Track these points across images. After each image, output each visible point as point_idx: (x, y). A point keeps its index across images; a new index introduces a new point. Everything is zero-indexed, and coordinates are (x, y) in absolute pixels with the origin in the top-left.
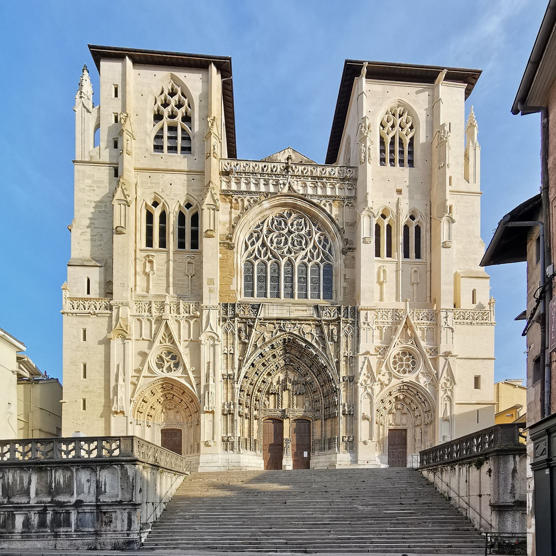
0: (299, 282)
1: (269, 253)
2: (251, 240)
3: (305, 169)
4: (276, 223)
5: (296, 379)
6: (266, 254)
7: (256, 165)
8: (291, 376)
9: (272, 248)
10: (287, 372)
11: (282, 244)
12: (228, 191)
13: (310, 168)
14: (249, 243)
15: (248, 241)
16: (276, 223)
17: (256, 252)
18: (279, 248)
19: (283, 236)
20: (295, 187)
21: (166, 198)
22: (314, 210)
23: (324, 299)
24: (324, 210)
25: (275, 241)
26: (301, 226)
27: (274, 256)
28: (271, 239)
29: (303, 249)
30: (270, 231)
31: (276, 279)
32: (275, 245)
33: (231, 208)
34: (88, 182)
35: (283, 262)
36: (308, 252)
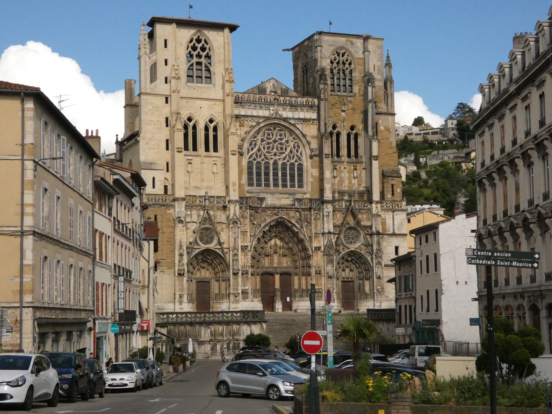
0: (282, 176)
2: (251, 147)
3: (285, 99)
4: (266, 134)
5: (282, 244)
6: (260, 156)
7: (255, 96)
8: (278, 242)
9: (264, 152)
10: (275, 240)
11: (271, 149)
12: (239, 115)
13: (288, 98)
14: (250, 148)
15: (250, 147)
16: (266, 134)
17: (254, 156)
18: (269, 153)
20: (280, 113)
21: (198, 118)
22: (292, 128)
23: (298, 188)
24: (298, 129)
25: (266, 146)
27: (266, 158)
28: (264, 146)
30: (262, 140)
31: (267, 174)
32: (266, 150)
33: (240, 126)
34: (150, 107)
35: (272, 162)
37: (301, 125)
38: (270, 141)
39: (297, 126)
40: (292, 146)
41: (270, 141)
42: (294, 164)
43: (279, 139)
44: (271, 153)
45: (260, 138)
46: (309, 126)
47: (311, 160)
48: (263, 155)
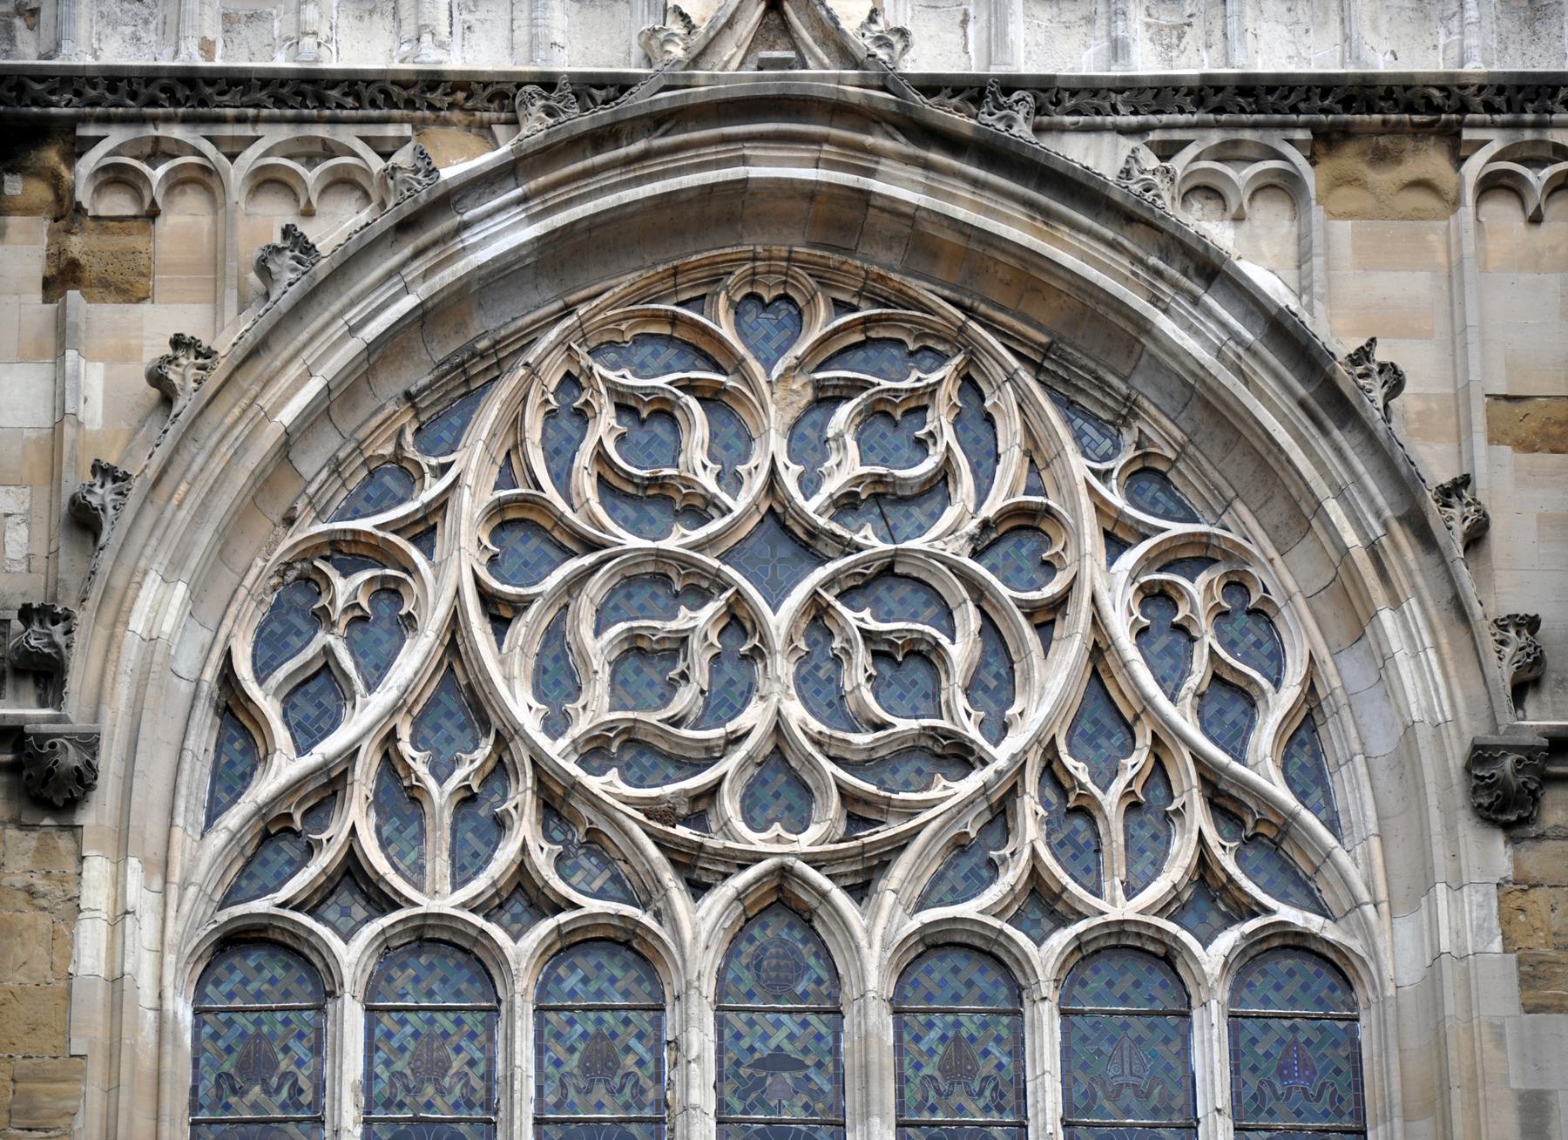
1: (526, 828)
4: (605, 424)
14: (269, 705)
15: (262, 672)
16: (605, 424)
19: (699, 596)
26: (922, 446)
29: (961, 756)
36: (1030, 808)
37: (1273, 221)
38: (678, 539)
39: (1218, 233)
40: (1121, 627)
41: (678, 539)
42: (1167, 958)
43: (846, 504)
44: (710, 756)
45: (472, 505)
46: (1434, 234)
47: (1498, 856)
48: (522, 797)
